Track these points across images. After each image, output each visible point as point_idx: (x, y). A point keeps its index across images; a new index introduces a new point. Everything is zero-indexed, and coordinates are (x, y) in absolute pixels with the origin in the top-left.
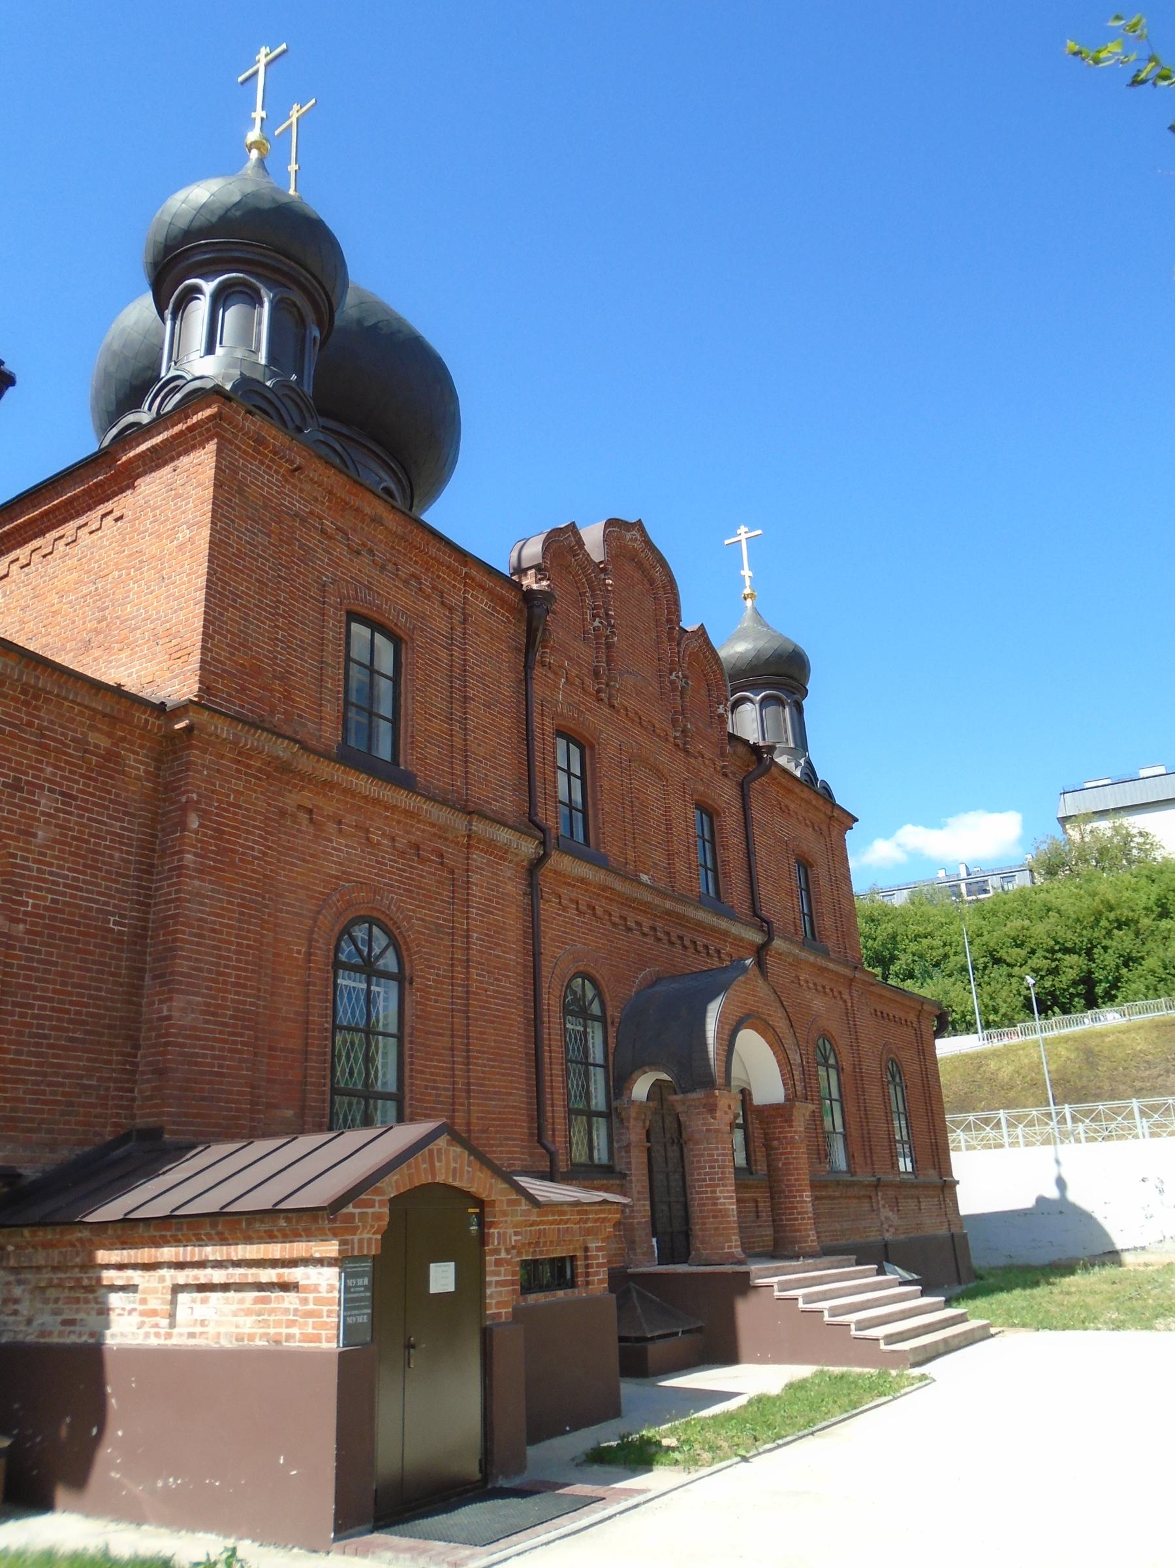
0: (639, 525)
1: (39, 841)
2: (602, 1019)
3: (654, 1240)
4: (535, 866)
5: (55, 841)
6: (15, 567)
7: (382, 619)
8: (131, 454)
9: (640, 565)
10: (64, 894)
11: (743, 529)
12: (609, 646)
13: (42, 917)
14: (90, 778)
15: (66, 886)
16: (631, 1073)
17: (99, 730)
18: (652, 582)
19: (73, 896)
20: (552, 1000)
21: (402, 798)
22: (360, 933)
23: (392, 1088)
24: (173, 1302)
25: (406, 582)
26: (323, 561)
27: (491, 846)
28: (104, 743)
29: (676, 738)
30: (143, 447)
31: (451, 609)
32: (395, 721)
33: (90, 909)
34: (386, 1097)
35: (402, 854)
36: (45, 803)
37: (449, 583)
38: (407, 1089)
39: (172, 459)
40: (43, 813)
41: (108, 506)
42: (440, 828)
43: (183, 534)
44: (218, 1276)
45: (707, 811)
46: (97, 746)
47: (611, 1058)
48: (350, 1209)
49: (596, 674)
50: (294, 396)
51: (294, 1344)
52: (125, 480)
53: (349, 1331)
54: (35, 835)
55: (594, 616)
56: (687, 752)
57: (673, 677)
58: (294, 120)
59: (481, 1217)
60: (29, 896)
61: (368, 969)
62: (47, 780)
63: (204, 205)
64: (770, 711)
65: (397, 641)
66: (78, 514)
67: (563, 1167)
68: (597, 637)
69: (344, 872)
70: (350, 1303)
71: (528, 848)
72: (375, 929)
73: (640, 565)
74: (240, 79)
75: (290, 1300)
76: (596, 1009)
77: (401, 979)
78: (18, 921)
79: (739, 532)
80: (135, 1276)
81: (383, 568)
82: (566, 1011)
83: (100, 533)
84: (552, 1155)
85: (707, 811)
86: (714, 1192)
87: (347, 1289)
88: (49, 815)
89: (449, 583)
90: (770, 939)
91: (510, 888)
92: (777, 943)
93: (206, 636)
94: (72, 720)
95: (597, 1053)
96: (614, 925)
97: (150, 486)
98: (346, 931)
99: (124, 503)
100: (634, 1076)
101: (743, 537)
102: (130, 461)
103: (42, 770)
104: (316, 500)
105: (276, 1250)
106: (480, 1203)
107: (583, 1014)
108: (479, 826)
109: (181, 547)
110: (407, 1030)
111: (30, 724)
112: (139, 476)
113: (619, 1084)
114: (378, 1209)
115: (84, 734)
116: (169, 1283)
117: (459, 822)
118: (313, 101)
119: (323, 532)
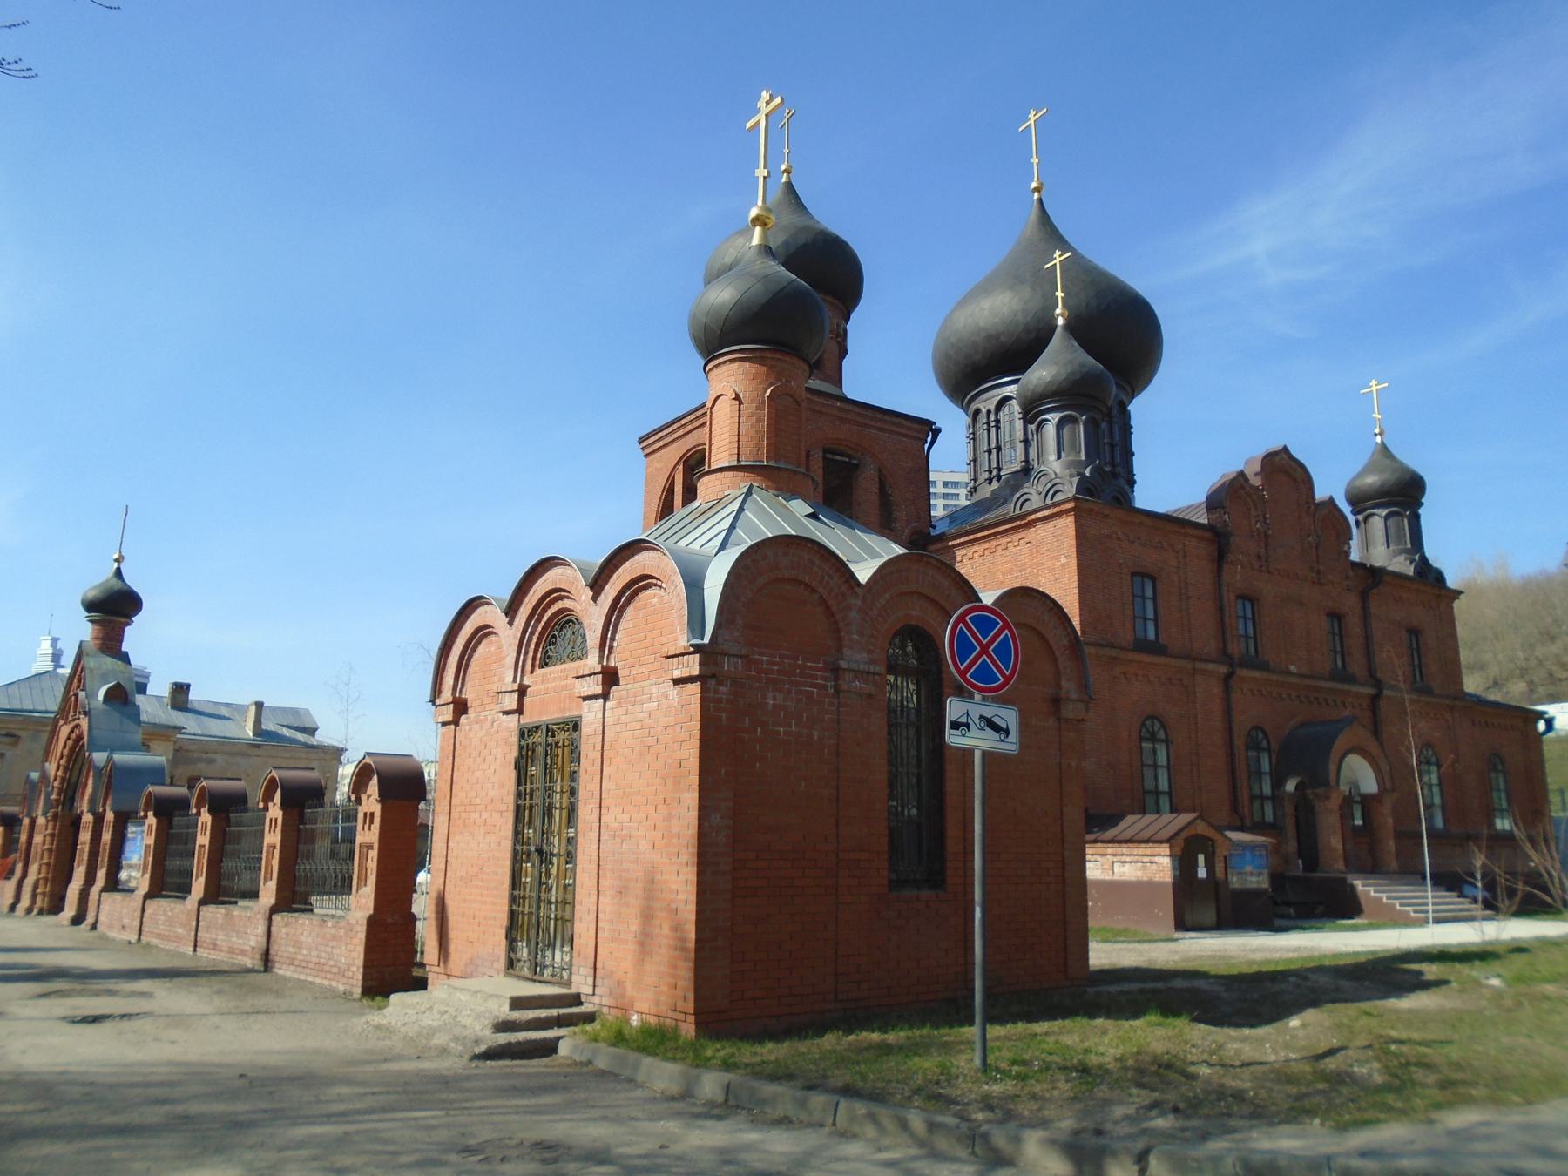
2: (1269, 750)
3: (1300, 862)
4: (1228, 677)
11: (1374, 383)
12: (1267, 537)
18: (1295, 480)
20: (1239, 743)
21: (1162, 660)
22: (1148, 723)
23: (1167, 790)
24: (1113, 866)
29: (1313, 577)
32: (1156, 621)
34: (1164, 793)
38: (1173, 789)
43: (1063, 560)
44: (1128, 859)
45: (1336, 616)
49: (1259, 557)
51: (1157, 879)
53: (1174, 877)
55: (1257, 522)
56: (1321, 584)
57: (1310, 539)
58: (1032, 121)
59: (1213, 846)
61: (1153, 738)
63: (1049, 381)
64: (1391, 522)
65: (1154, 579)
67: (1248, 823)
68: (1258, 535)
70: (1174, 868)
71: (1223, 669)
72: (1155, 721)
75: (1154, 867)
76: (1264, 744)
77: (1167, 742)
79: (1371, 384)
80: (1099, 858)
82: (1248, 748)
83: (1019, 548)
84: (1242, 819)
85: (1336, 616)
90: (1381, 692)
92: (1386, 692)
93: (1081, 609)
95: (1266, 767)
97: (1042, 532)
98: (1143, 724)
99: (1030, 534)
101: (1374, 388)
105: (1148, 851)
106: (1212, 841)
107: (1258, 748)
108: (1198, 665)
110: (1171, 763)
113: (1278, 783)
114: (1180, 841)
116: (1111, 860)
117: (1188, 665)
118: (1045, 110)
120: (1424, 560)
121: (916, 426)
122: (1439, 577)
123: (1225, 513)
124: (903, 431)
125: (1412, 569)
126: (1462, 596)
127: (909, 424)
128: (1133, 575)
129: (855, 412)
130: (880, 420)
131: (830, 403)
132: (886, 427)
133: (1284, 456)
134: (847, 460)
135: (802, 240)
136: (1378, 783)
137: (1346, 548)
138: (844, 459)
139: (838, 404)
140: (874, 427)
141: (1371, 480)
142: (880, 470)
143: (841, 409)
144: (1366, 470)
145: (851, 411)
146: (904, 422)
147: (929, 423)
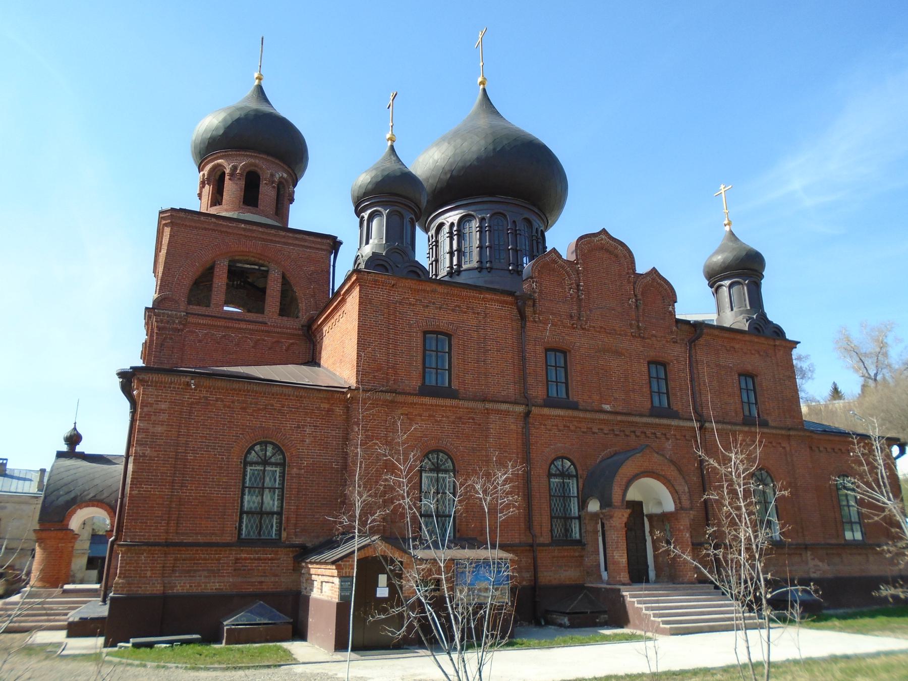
0: (604, 231)
1: (307, 443)
2: (577, 476)
4: (528, 414)
5: (312, 442)
7: (440, 330)
9: (607, 251)
10: (316, 458)
11: (722, 186)
13: (310, 467)
14: (323, 419)
15: (317, 455)
16: (587, 499)
17: (325, 403)
18: (616, 256)
19: (319, 458)
24: (322, 586)
25: (453, 310)
26: (410, 315)
27: (499, 412)
28: (327, 406)
31: (478, 313)
33: (326, 462)
35: (453, 423)
36: (308, 430)
37: (476, 303)
40: (308, 434)
42: (471, 409)
46: (324, 408)
47: (580, 493)
48: (340, 562)
50: (398, 251)
54: (305, 441)
55: (571, 288)
57: (630, 302)
60: (305, 461)
62: (308, 423)
64: (735, 289)
68: (572, 298)
69: (424, 434)
73: (607, 251)
78: (302, 469)
81: (440, 308)
86: (613, 553)
87: (341, 585)
88: (310, 434)
89: (476, 303)
91: (513, 427)
94: (314, 402)
95: (574, 491)
96: (583, 432)
100: (588, 501)
101: (723, 191)
104: (405, 293)
111: (301, 406)
113: (583, 505)
115: (320, 405)
117: (480, 405)
119: (410, 304)
120: (763, 316)
122: (778, 332)
123: (533, 283)
124: (306, 244)
125: (747, 325)
126: (798, 346)
127: (312, 238)
128: (425, 333)
129: (258, 231)
130: (284, 237)
131: (234, 225)
132: (290, 241)
133: (603, 237)
134: (257, 267)
135: (236, 116)
136: (675, 502)
137: (670, 309)
138: (253, 267)
139: (243, 226)
140: (279, 242)
141: (719, 258)
143: (244, 229)
144: (717, 252)
145: (255, 230)
146: (307, 237)
147: (334, 238)
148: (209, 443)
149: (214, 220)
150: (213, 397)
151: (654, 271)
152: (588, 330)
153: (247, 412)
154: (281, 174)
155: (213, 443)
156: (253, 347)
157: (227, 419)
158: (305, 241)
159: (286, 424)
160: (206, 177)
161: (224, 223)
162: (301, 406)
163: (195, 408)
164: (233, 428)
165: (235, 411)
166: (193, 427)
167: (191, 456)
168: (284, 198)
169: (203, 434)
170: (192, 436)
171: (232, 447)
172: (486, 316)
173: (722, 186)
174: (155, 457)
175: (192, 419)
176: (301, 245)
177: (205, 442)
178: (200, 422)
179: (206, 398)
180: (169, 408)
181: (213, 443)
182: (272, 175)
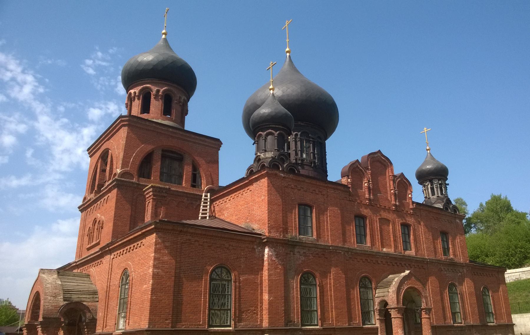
6: (231, 198)
8: (251, 178)
14: (249, 253)
25: (312, 193)
26: (292, 195)
30: (254, 177)
31: (324, 195)
37: (323, 189)
39: (259, 180)
41: (248, 187)
43: (263, 197)
52: (251, 183)
66: (242, 189)
74: (267, 69)
83: (247, 193)
89: (323, 189)
102: (251, 180)
103: (241, 254)
109: (262, 200)
111: (239, 246)
112: (253, 182)
121: (213, 142)
124: (206, 144)
129: (180, 134)
132: (197, 141)
133: (379, 154)
139: (171, 130)
142: (193, 161)
146: (207, 140)
148: (191, 267)
149: (154, 125)
150: (193, 240)
151: (402, 174)
152: (374, 206)
153: (211, 249)
154: (184, 97)
155: (194, 267)
156: (176, 206)
157: (201, 253)
158: (206, 142)
159: (231, 256)
160: (137, 94)
161: (160, 127)
162: (239, 246)
163: (184, 246)
164: (204, 258)
165: (205, 248)
166: (183, 257)
167: (182, 275)
168: (184, 112)
169: (189, 261)
170: (183, 263)
171: (204, 270)
172: (328, 197)
173: (425, 129)
174: (164, 276)
175: (182, 252)
176: (204, 144)
177: (190, 267)
178: (187, 254)
179: (189, 240)
180: (170, 245)
181: (194, 267)
182: (180, 98)
